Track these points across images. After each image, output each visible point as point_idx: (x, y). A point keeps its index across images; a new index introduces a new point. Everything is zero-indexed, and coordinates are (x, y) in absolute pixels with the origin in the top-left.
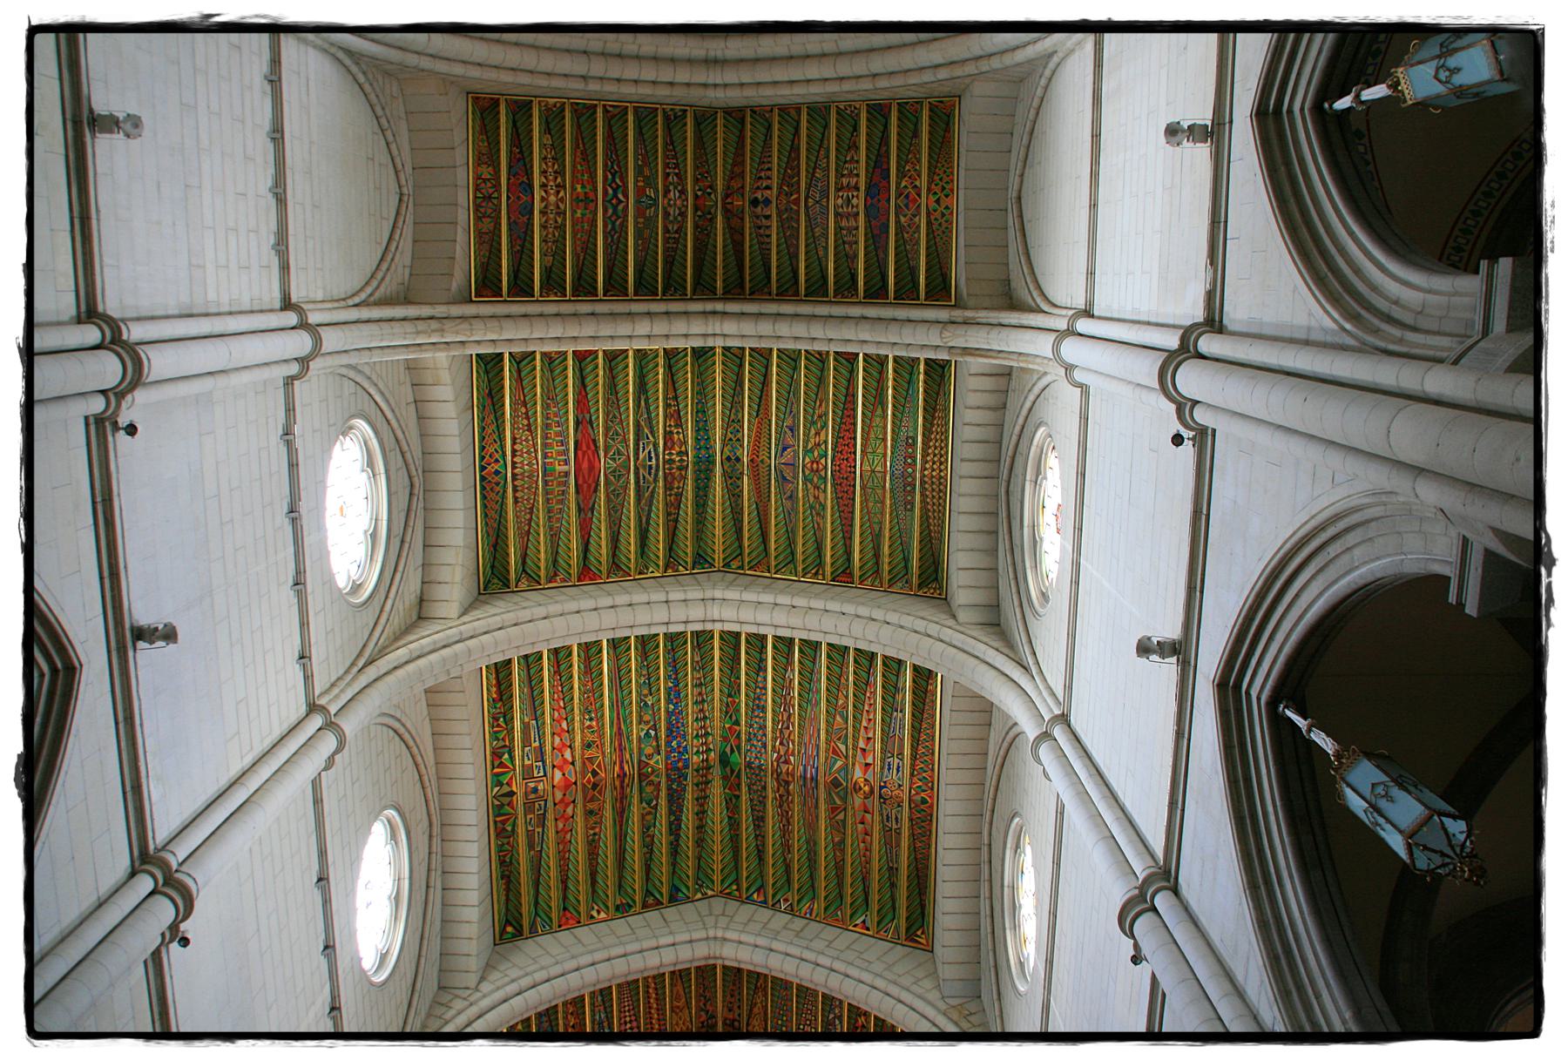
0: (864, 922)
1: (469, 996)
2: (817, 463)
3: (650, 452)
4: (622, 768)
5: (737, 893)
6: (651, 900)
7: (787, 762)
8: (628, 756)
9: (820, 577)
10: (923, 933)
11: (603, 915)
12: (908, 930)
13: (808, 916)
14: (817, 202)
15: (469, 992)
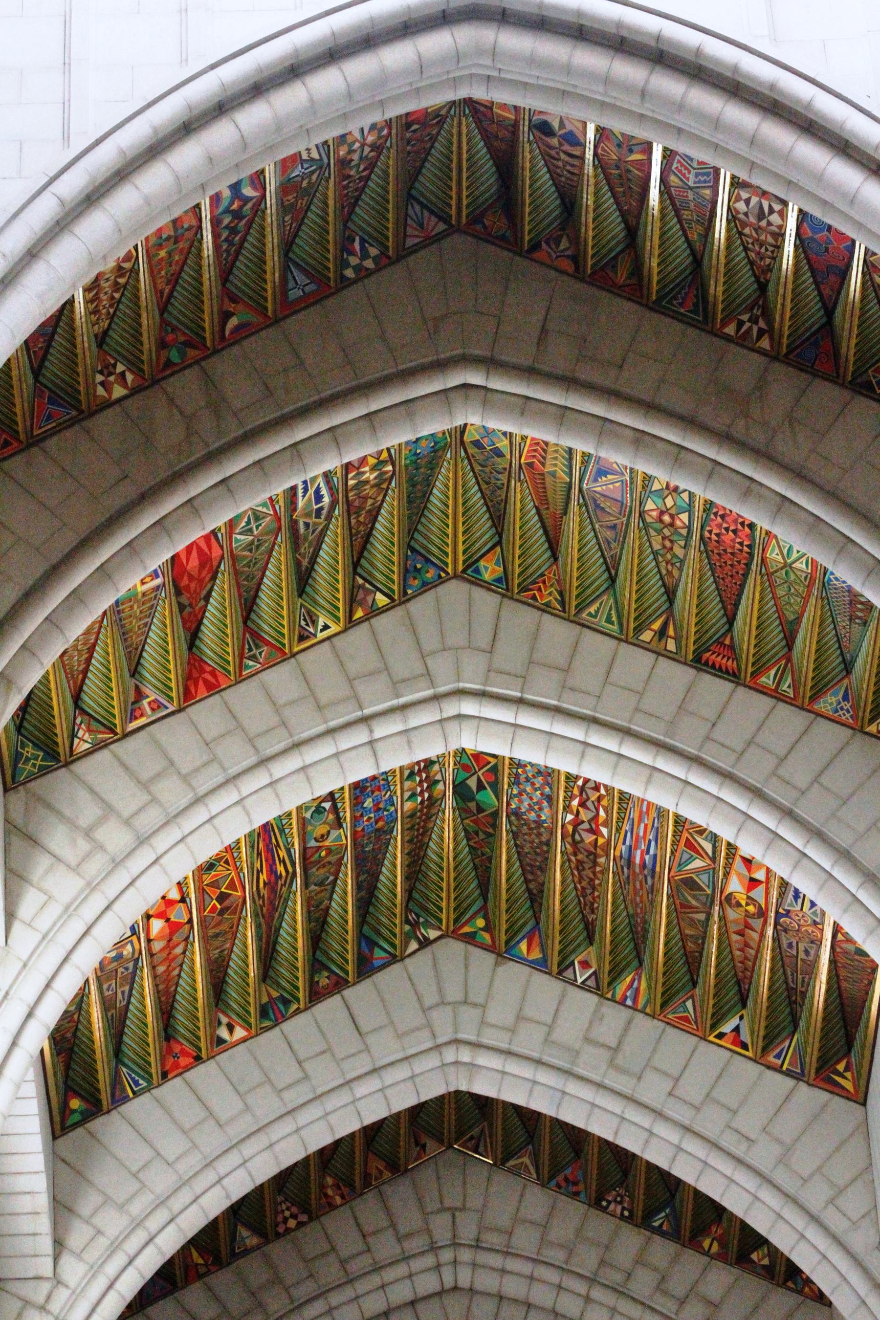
0: (737, 1029)
1: (49, 1298)
2: (672, 516)
3: (318, 491)
4: (272, 871)
5: (486, 937)
6: (323, 980)
7: (595, 831)
8: (283, 853)
9: (671, 645)
10: (847, 1069)
11: (240, 1033)
12: (818, 1070)
13: (629, 1002)
14: (691, 188)
15: (46, 1287)
